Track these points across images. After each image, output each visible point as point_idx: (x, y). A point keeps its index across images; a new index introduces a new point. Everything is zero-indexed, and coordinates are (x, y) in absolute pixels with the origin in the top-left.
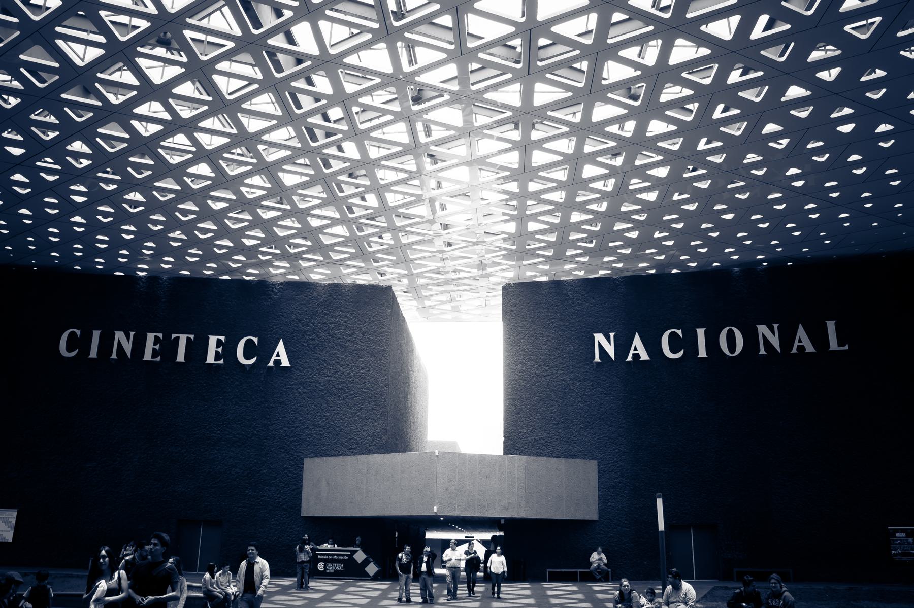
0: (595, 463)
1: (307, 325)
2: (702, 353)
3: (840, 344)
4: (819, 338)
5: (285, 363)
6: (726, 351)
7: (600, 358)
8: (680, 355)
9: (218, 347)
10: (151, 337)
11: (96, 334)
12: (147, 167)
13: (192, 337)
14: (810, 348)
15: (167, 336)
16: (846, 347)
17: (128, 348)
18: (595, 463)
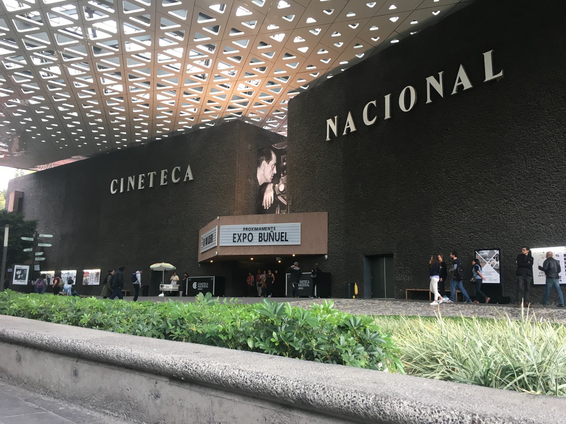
3: (495, 72)
4: (476, 73)
5: (191, 178)
10: (140, 176)
15: (146, 175)
16: (501, 74)
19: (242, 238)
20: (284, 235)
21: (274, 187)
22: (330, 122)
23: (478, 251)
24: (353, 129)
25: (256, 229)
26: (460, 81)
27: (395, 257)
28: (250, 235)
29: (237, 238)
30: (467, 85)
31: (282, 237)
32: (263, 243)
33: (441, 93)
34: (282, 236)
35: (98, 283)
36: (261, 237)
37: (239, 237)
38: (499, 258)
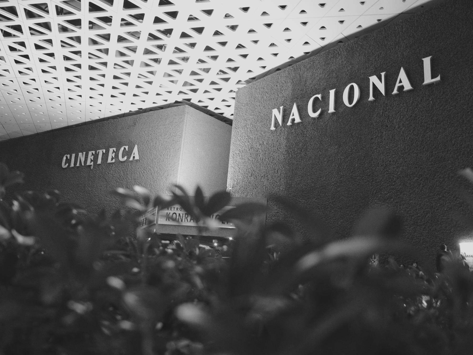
3: (433, 77)
10: (90, 153)
16: (438, 78)
22: (275, 111)
24: (298, 120)
26: (401, 82)
30: (407, 86)
33: (383, 92)
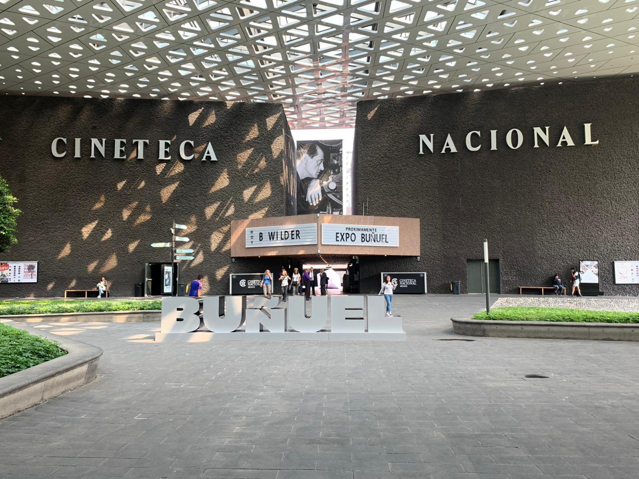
0: (419, 220)
1: (227, 132)
2: (494, 147)
4: (579, 136)
6: (511, 147)
7: (423, 151)
8: (479, 147)
9: (166, 147)
10: (118, 142)
11: (78, 141)
12: (107, 14)
13: (147, 141)
14: (570, 143)
16: (597, 142)
17: (102, 150)
18: (419, 220)
19: (344, 237)
20: (384, 237)
21: (321, 184)
23: (582, 261)
25: (359, 230)
27: (501, 262)
28: (353, 235)
29: (340, 237)
31: (383, 238)
32: (365, 244)
34: (383, 237)
35: (34, 280)
36: (363, 238)
37: (342, 237)
38: (598, 266)
